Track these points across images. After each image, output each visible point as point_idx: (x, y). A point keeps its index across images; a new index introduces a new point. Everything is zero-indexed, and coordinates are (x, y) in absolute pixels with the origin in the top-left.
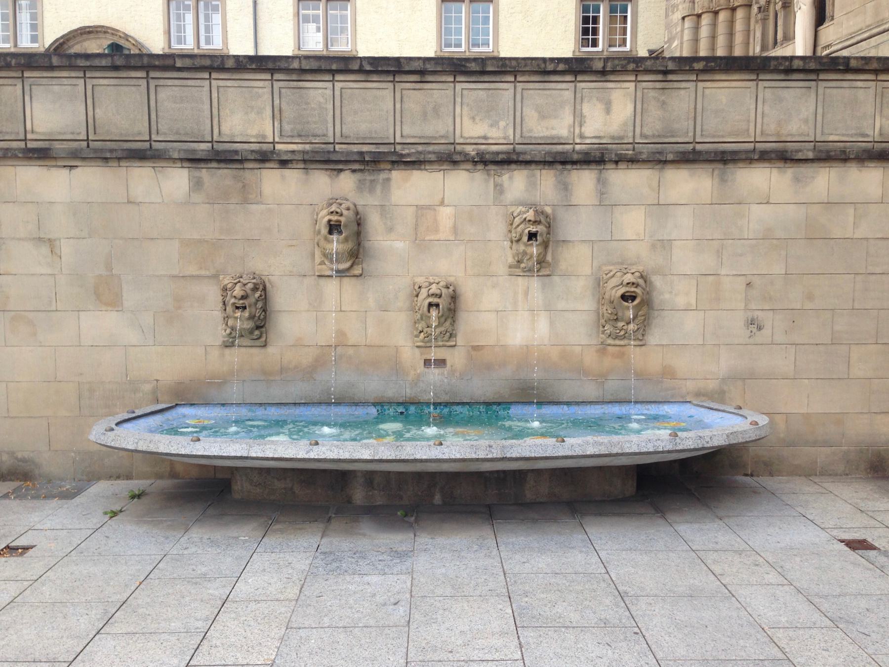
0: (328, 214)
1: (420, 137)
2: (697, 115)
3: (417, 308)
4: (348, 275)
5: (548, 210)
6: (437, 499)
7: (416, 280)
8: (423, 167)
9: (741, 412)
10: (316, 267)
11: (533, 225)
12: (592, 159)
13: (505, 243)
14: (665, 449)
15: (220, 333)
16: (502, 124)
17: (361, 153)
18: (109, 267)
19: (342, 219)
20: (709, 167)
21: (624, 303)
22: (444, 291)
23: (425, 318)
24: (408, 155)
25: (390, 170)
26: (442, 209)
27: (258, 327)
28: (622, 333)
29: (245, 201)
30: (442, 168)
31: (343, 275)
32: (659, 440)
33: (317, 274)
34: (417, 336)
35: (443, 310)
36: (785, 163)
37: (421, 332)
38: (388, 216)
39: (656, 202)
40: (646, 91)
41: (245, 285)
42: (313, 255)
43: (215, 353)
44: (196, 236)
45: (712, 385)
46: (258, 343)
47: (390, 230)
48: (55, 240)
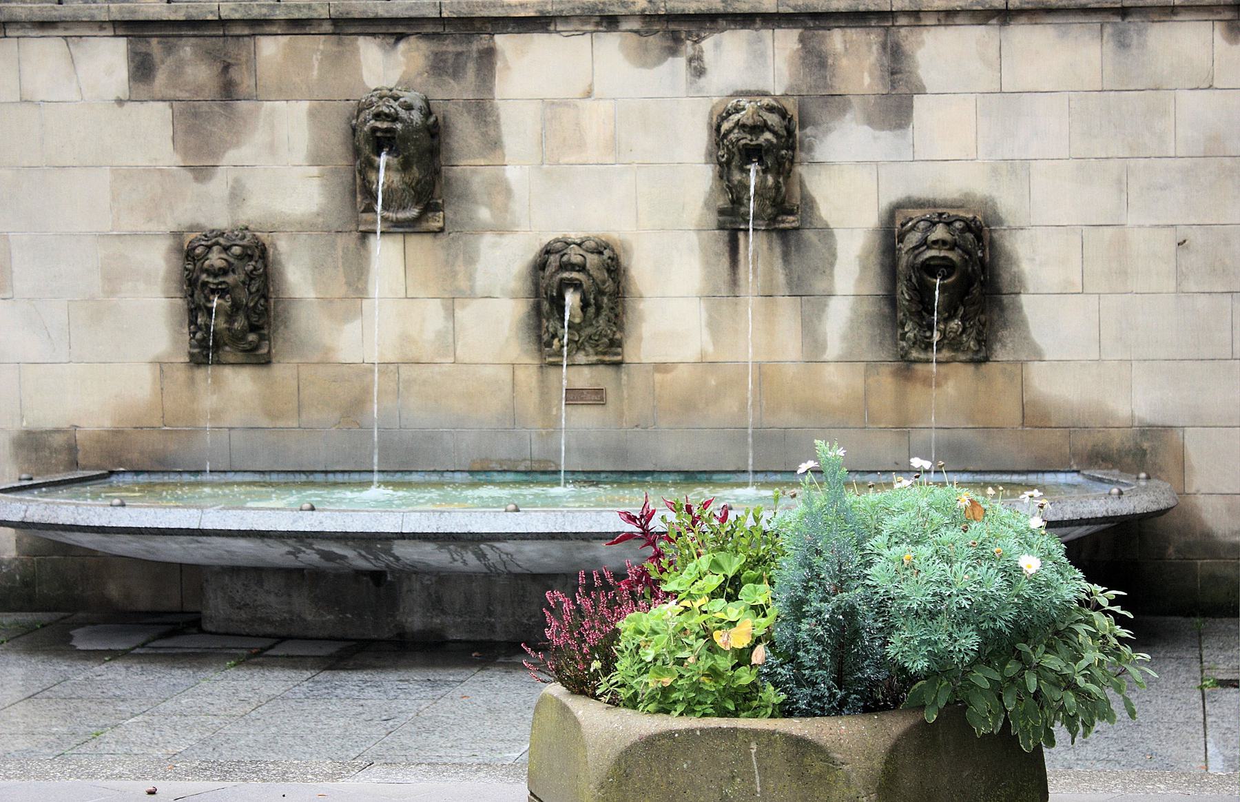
22: (592, 260)
27: (254, 328)
38: (489, 119)
39: (996, 88)
44: (142, 161)
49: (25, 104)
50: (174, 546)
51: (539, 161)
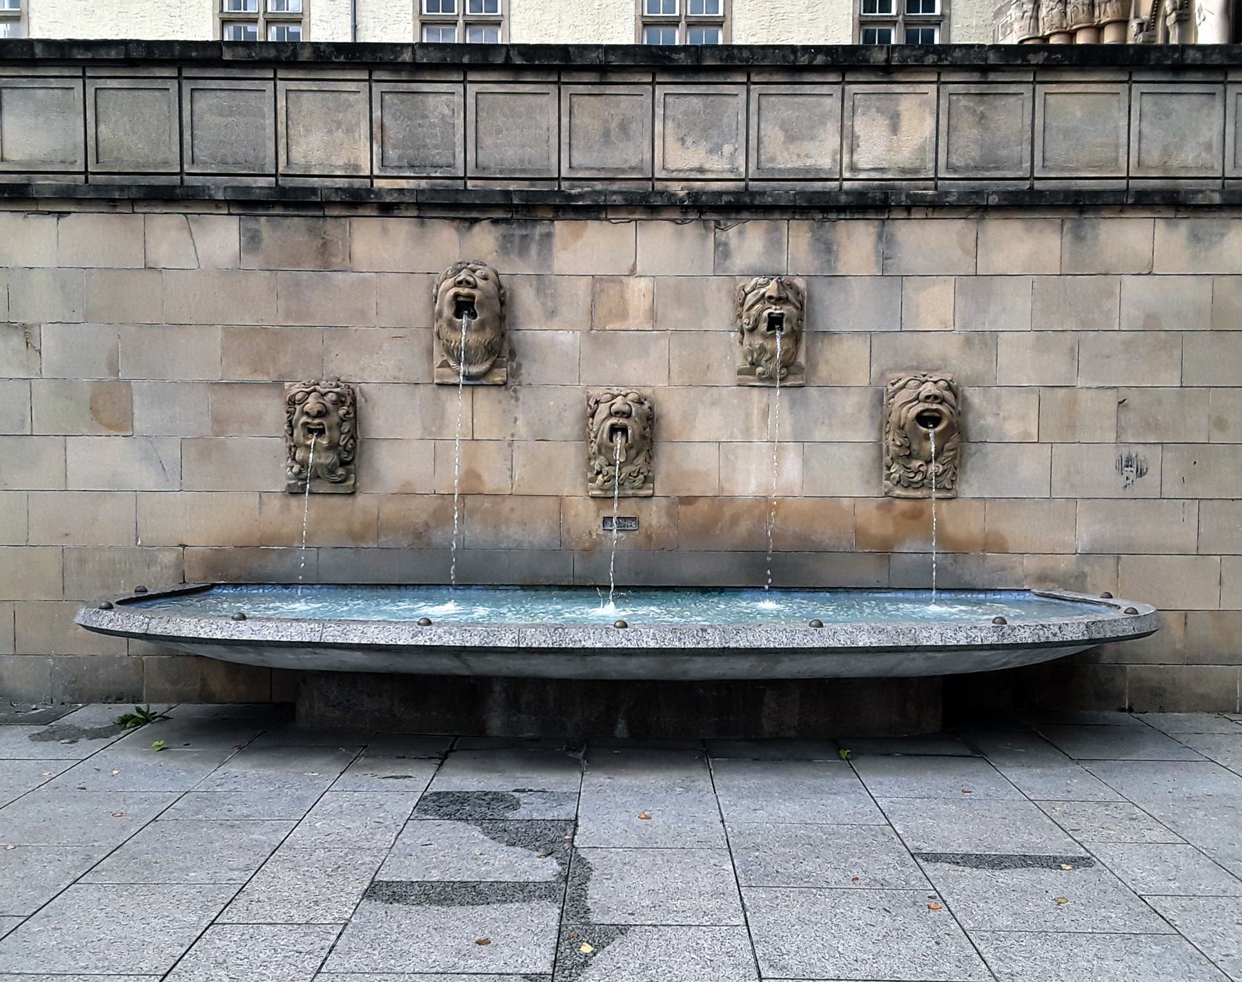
0: (455, 286)
1: (599, 170)
2: (1036, 135)
3: (592, 435)
4: (484, 382)
5: (800, 283)
6: (621, 729)
7: (591, 393)
8: (603, 216)
9: (1111, 601)
10: (435, 370)
11: (775, 304)
12: (870, 202)
13: (732, 334)
14: (986, 642)
15: (284, 474)
16: (727, 149)
17: (507, 194)
18: (114, 369)
19: (476, 293)
20: (1056, 217)
21: (921, 428)
23: (605, 450)
24: (581, 196)
25: (552, 221)
26: (632, 281)
27: (343, 464)
28: (919, 477)
29: (326, 267)
30: (631, 217)
31: (477, 383)
32: (976, 627)
33: (436, 381)
34: (593, 480)
35: (633, 437)
36: (1178, 211)
37: (599, 473)
38: (548, 292)
39: (972, 271)
40: (955, 98)
41: (323, 395)
42: (431, 352)
43: (274, 505)
45: (1065, 564)
46: (341, 489)
47: (552, 313)
48: (32, 326)
49: (148, 271)
50: (290, 656)
51: (588, 328)
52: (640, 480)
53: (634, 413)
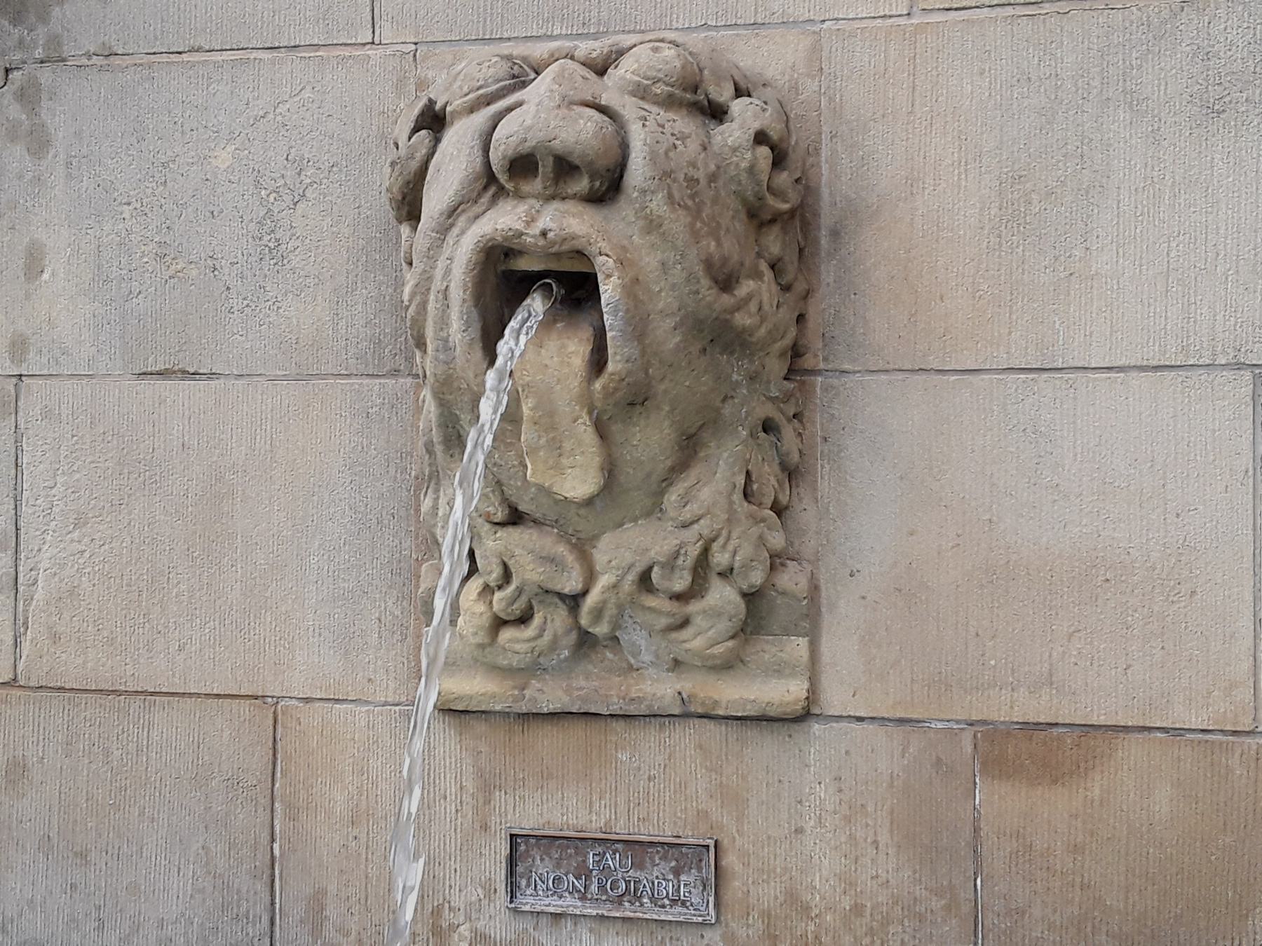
35: (638, 328)
52: (715, 614)
53: (638, 171)
